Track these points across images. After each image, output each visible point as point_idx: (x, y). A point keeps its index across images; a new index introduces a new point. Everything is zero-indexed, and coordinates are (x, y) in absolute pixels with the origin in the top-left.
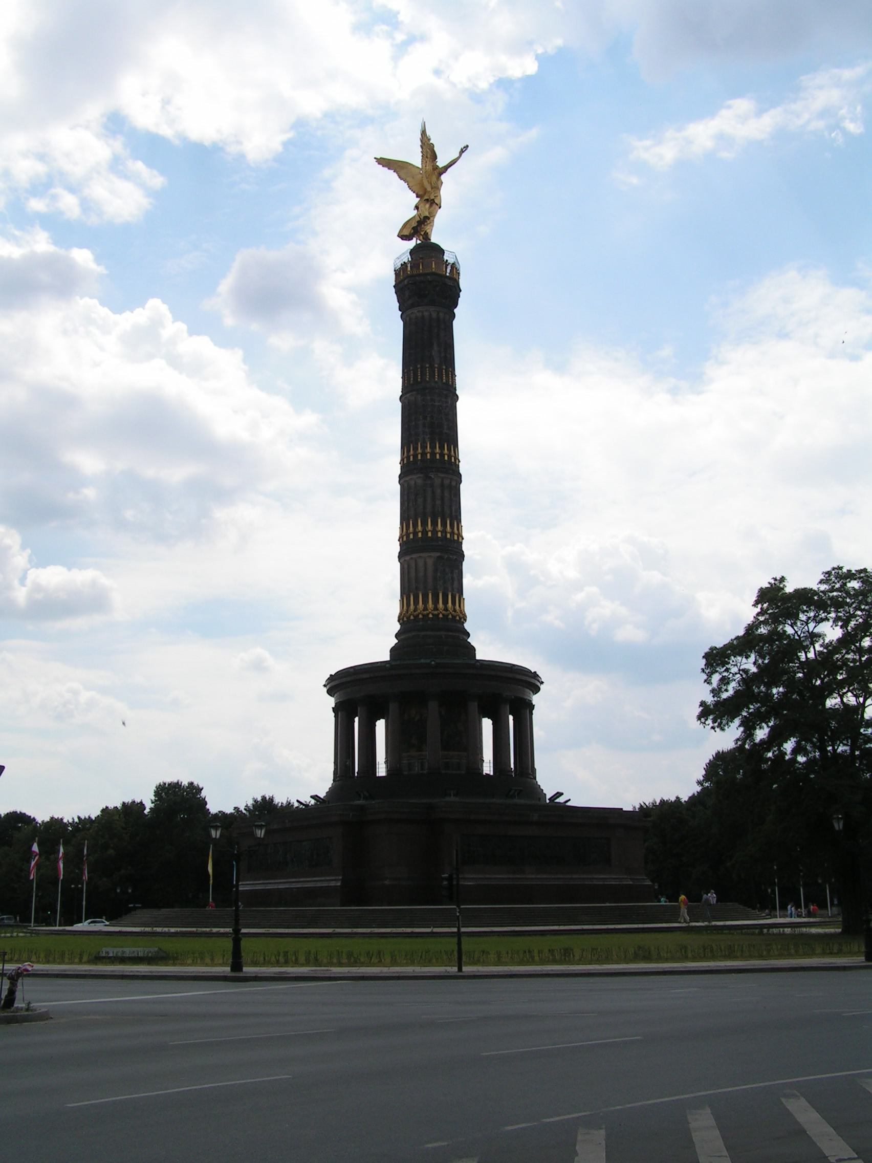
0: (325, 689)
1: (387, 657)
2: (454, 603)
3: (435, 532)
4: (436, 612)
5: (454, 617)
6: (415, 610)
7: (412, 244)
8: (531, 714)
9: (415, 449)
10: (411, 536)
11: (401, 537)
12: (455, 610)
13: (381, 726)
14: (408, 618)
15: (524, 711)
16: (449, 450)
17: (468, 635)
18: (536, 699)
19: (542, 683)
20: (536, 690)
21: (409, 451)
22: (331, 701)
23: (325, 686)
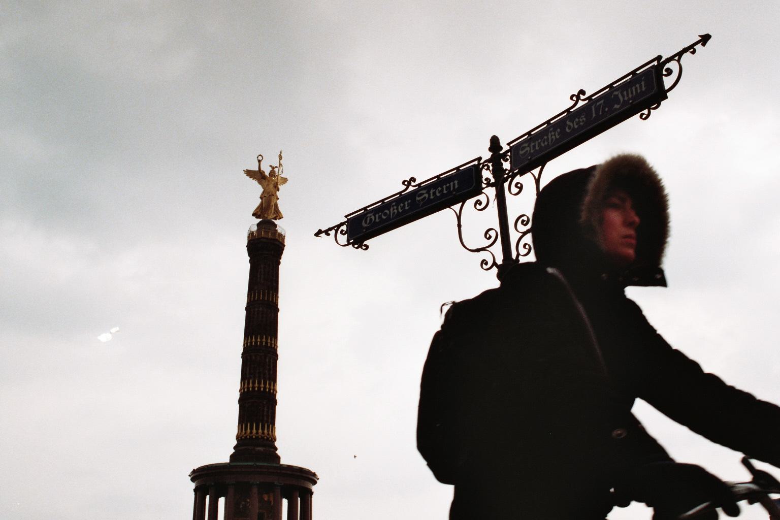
0: (190, 478)
1: (227, 460)
4: (257, 435)
5: (268, 439)
6: (245, 433)
7: (259, 220)
8: (311, 497)
9: (251, 339)
10: (246, 390)
11: (240, 390)
12: (268, 434)
13: (222, 501)
15: (307, 495)
16: (271, 340)
17: (276, 449)
18: (314, 488)
19: (318, 479)
20: (315, 483)
22: (193, 485)
23: (189, 476)
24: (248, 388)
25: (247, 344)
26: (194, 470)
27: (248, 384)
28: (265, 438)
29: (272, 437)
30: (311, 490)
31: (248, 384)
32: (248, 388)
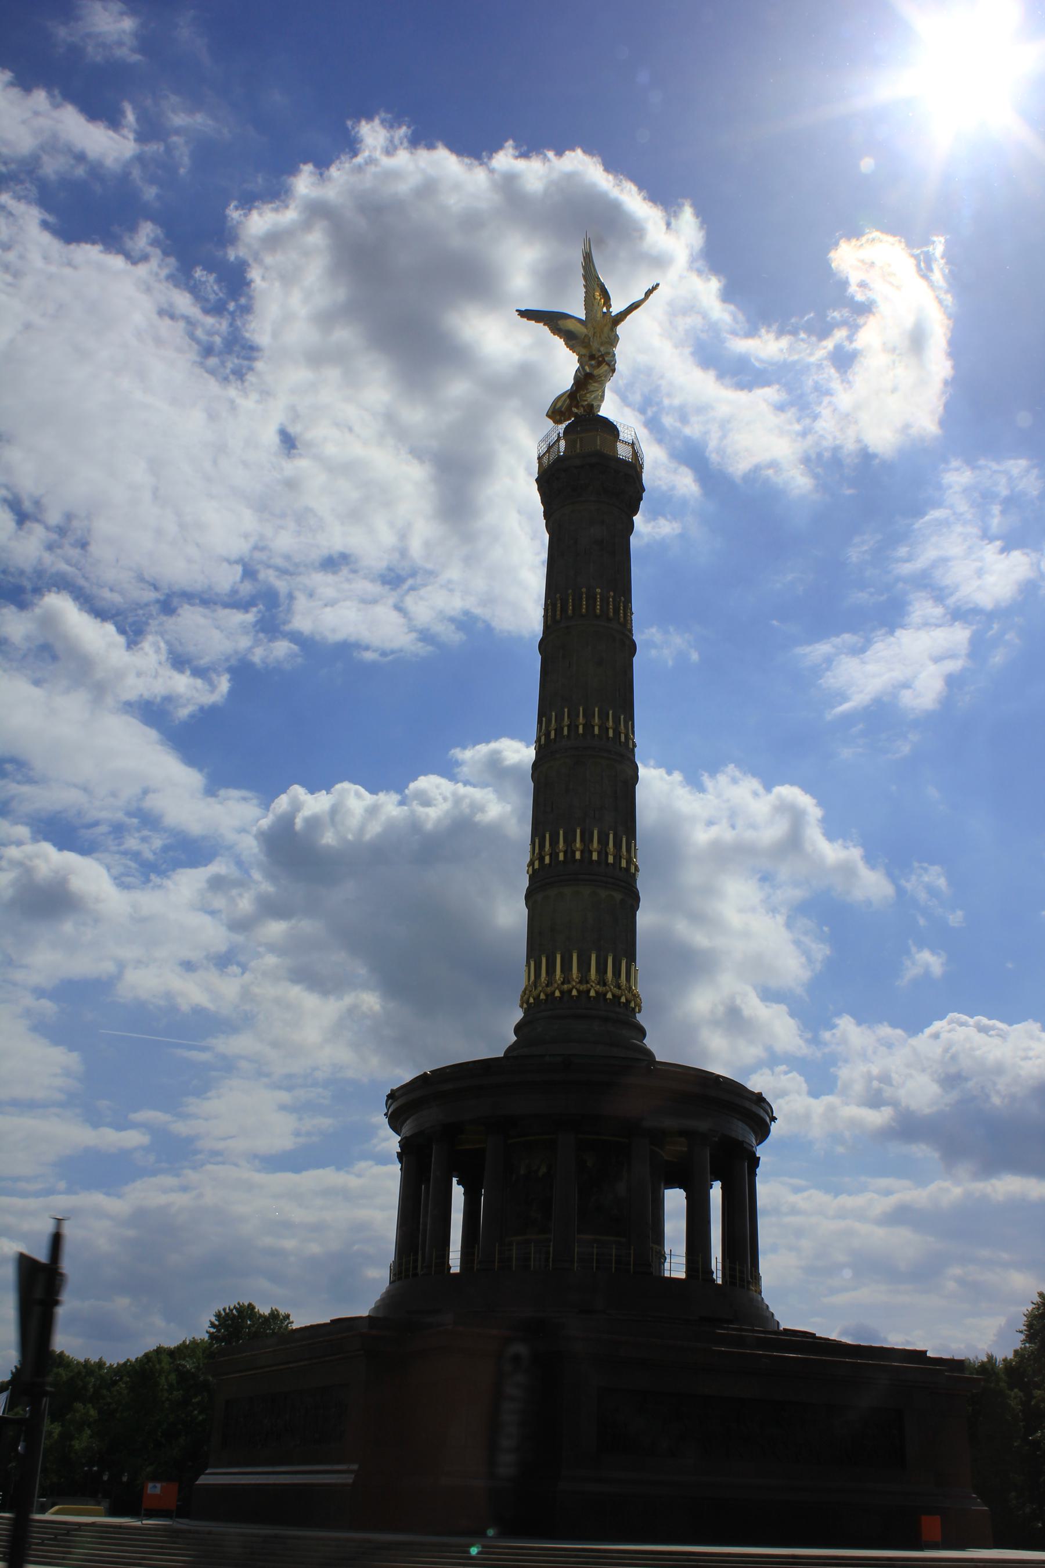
2: (617, 973)
3: (586, 851)
8: (753, 1174)
10: (547, 860)
11: (531, 863)
12: (619, 987)
14: (537, 998)
15: (738, 1170)
17: (642, 1032)
18: (761, 1151)
21: (549, 722)
24: (554, 855)
25: (547, 734)
26: (392, 1090)
27: (554, 842)
28: (609, 996)
29: (630, 996)
30: (754, 1154)
31: (554, 842)
32: (554, 855)
